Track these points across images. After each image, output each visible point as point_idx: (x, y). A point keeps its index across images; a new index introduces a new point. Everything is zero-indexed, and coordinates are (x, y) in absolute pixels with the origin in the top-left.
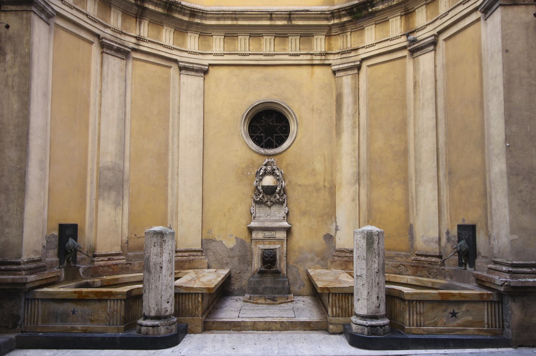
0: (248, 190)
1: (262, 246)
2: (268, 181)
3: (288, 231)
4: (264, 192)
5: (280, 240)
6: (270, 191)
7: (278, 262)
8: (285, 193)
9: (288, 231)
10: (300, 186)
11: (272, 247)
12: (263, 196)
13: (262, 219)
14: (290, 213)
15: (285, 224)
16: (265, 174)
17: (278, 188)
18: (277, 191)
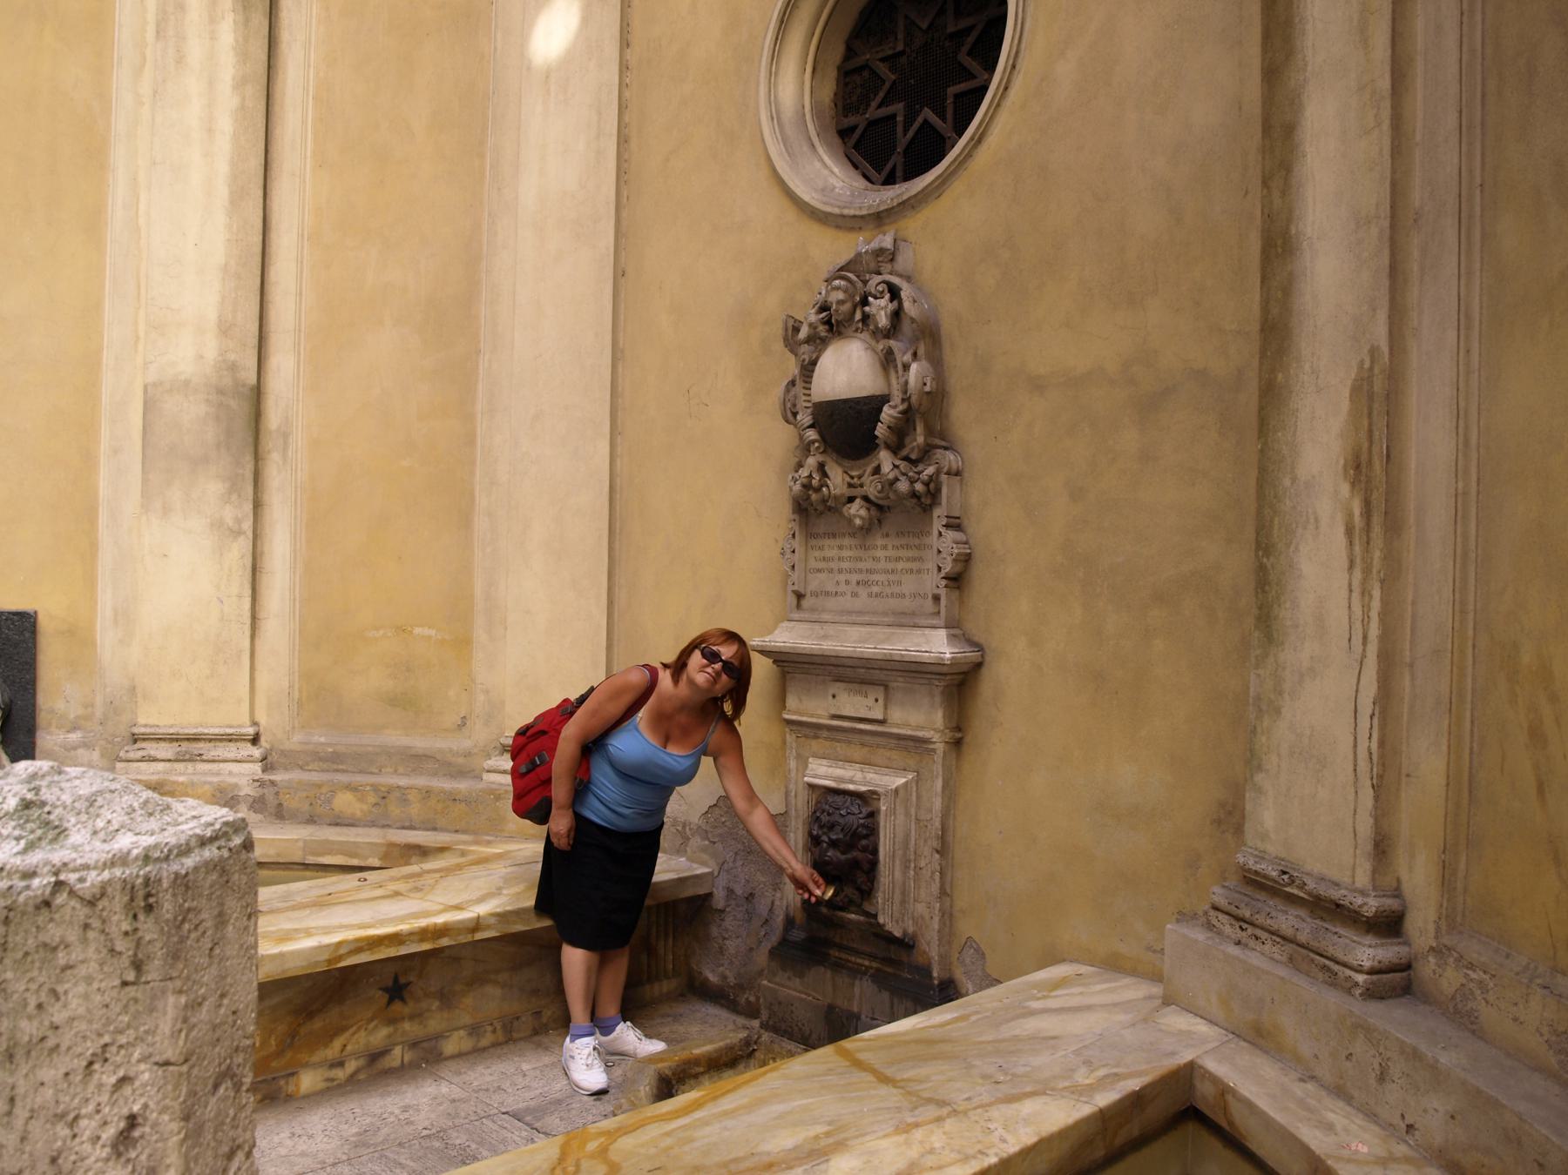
0: (780, 438)
1: (824, 772)
2: (847, 370)
3: (959, 685)
4: (823, 439)
5: (915, 745)
6: (846, 429)
7: (889, 873)
8: (941, 438)
9: (959, 685)
10: (1038, 385)
11: (855, 777)
12: (821, 467)
13: (831, 603)
14: (980, 575)
15: (937, 646)
16: (833, 326)
17: (888, 413)
18: (880, 430)
